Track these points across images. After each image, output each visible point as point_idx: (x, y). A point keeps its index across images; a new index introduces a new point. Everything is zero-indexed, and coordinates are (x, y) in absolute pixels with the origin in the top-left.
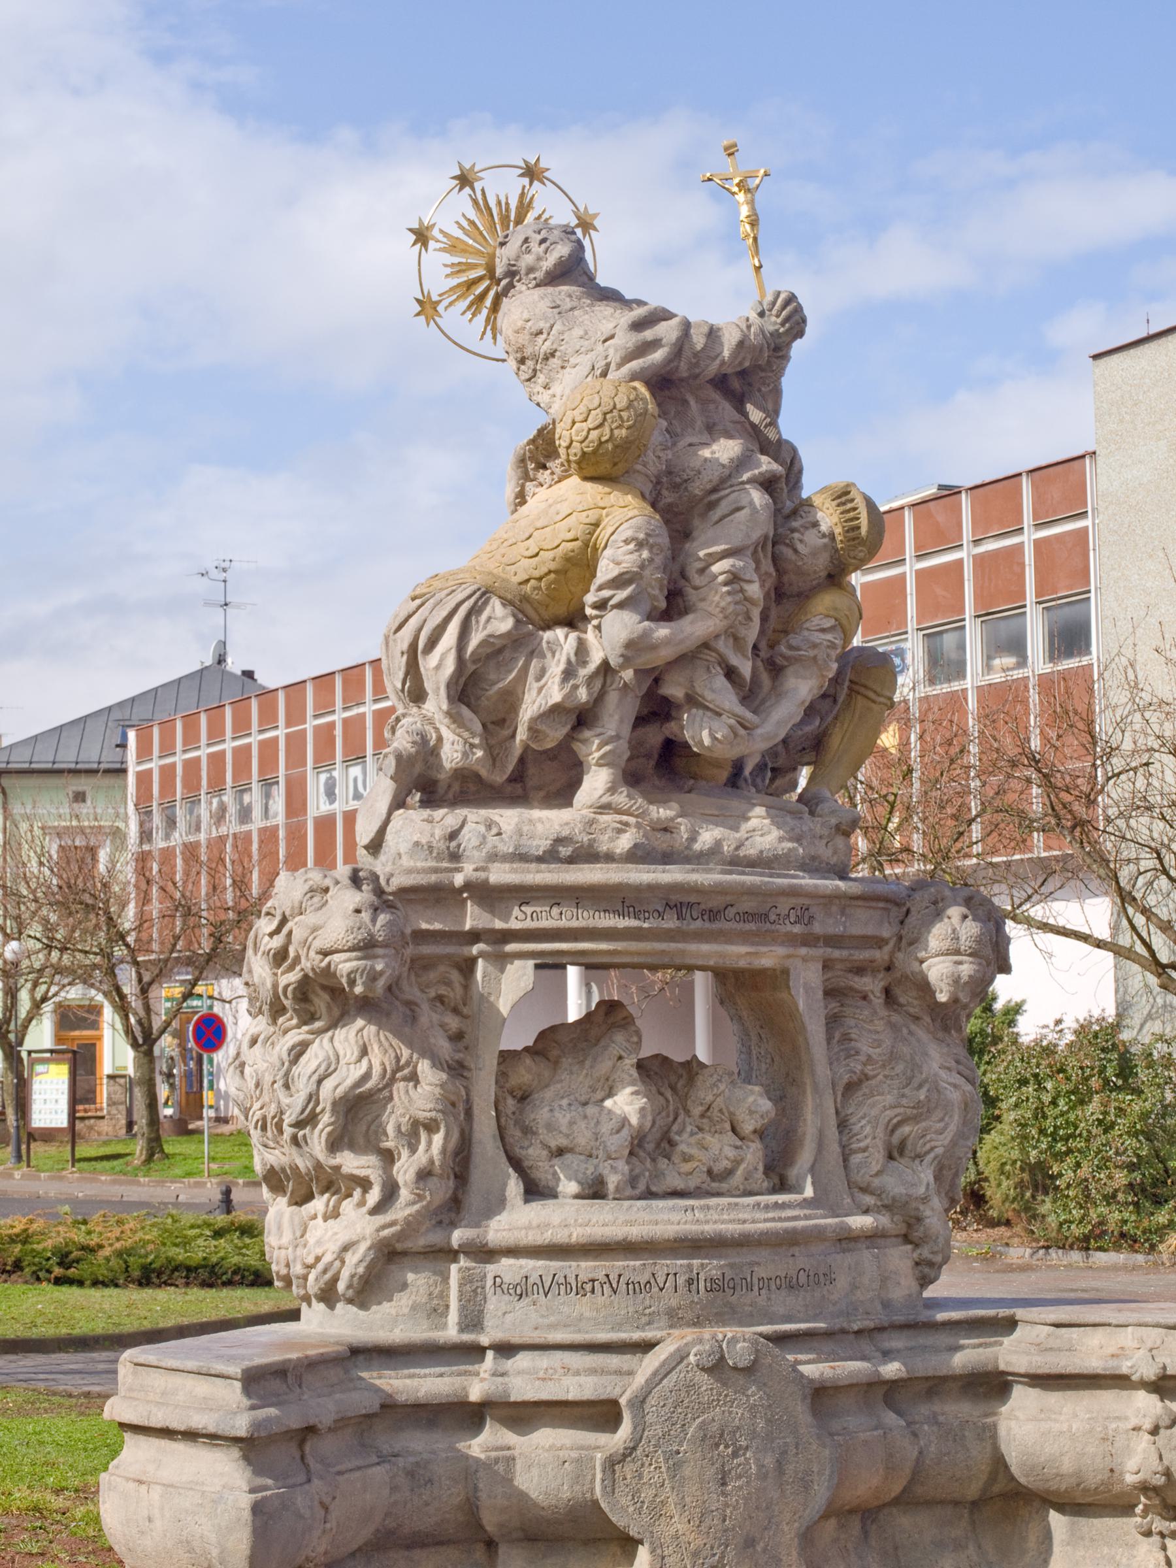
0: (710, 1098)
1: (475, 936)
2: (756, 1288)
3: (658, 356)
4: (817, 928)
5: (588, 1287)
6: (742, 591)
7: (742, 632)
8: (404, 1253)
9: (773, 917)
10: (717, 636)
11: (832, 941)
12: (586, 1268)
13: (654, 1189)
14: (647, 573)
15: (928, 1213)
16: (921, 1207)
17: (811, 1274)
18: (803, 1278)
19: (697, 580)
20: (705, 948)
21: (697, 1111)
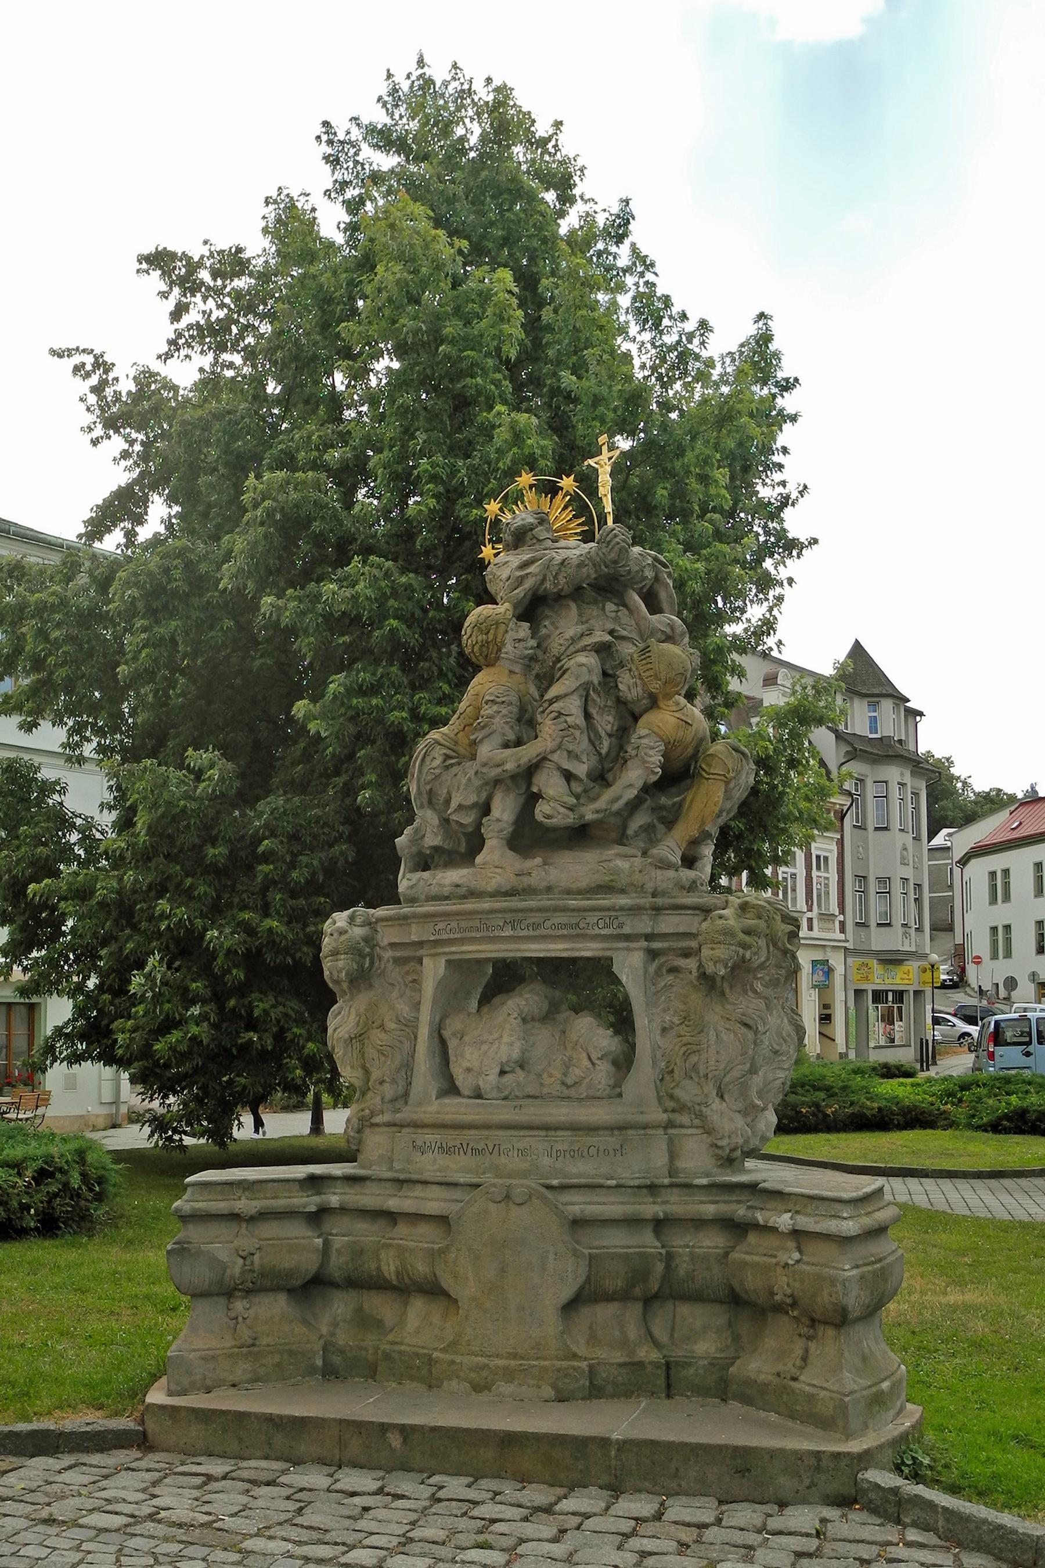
0: (575, 1038)
1: (420, 944)
2: (554, 1155)
3: (528, 584)
4: (627, 930)
5: (452, 1150)
6: (566, 722)
7: (571, 747)
8: (377, 1125)
9: (582, 925)
10: (553, 752)
11: (649, 937)
12: (451, 1138)
13: (517, 1094)
14: (497, 720)
15: (709, 1113)
16: (704, 1109)
17: (601, 1149)
18: (593, 1151)
19: (539, 719)
20: (533, 946)
21: (569, 1046)
